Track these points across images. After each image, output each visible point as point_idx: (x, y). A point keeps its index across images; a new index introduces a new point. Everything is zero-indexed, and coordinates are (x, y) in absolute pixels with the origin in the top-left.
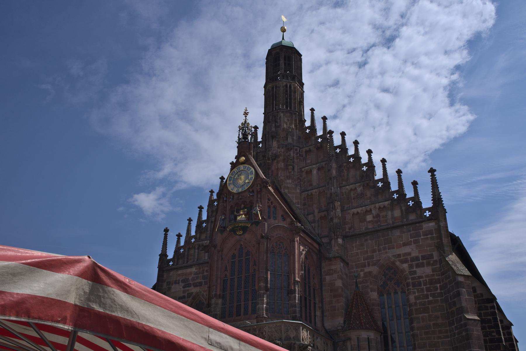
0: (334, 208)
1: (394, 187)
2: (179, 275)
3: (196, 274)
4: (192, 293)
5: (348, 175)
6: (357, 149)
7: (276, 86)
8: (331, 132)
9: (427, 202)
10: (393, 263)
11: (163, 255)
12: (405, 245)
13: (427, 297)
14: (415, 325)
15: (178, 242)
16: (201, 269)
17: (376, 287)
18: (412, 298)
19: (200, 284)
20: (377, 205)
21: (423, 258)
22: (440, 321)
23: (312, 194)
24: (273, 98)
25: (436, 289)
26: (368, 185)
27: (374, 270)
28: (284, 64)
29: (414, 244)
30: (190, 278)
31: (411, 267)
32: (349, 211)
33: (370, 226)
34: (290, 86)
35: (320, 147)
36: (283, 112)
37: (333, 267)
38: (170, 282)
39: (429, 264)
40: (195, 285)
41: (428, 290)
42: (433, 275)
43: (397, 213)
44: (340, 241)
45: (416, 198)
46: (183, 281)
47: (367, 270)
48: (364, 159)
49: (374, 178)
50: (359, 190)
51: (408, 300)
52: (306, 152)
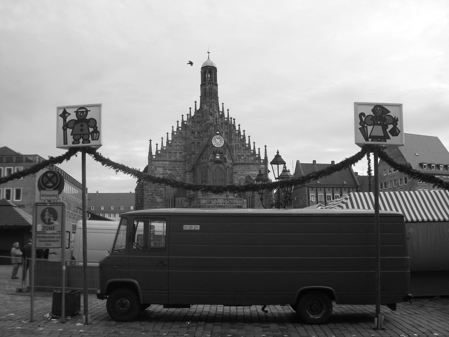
0: (233, 152)
1: (252, 149)
2: (160, 164)
3: (169, 165)
6: (239, 128)
9: (263, 157)
10: (250, 176)
11: (150, 152)
12: (254, 171)
14: (255, 198)
19: (172, 170)
27: (244, 177)
30: (166, 166)
40: (169, 170)
43: (252, 158)
45: (259, 154)
46: (163, 167)
47: (241, 177)
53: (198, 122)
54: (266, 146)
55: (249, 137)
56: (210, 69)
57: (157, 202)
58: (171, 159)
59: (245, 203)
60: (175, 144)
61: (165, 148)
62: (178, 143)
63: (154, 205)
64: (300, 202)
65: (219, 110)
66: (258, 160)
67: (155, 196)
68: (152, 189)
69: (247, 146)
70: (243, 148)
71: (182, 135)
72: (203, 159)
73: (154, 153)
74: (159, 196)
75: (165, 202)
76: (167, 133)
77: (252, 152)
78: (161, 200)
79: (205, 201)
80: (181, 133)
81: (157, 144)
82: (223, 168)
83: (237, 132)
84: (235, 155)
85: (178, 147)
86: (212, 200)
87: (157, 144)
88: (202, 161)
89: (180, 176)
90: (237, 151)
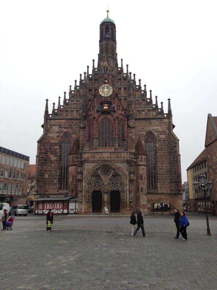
0: (131, 106)
1: (154, 103)
2: (56, 122)
3: (65, 123)
4: (63, 131)
5: (136, 94)
7: (108, 43)
8: (130, 73)
9: (166, 111)
10: (152, 132)
11: (47, 111)
12: (156, 126)
13: (163, 145)
14: (158, 154)
15: (54, 107)
16: (68, 121)
17: (144, 139)
18: (157, 145)
19: (67, 128)
20: (147, 109)
21: (163, 132)
22: (166, 154)
23: (121, 99)
24: (106, 49)
25: (166, 143)
26: (144, 99)
27: (144, 133)
28: (108, 30)
29: (160, 126)
30: (62, 124)
31: (158, 134)
32: (136, 109)
33: (143, 117)
34: (114, 45)
35: (125, 79)
36: (111, 58)
37: (132, 131)
38: (51, 125)
39: (164, 134)
40: (65, 128)
41: (163, 143)
42: (166, 138)
44: (133, 120)
45: (162, 109)
46: (58, 125)
47: (142, 133)
48: (143, 89)
49: (146, 97)
50: (140, 101)
51: (155, 146)
52: (119, 79)
53: (95, 80)
54: (169, 100)
55: (151, 91)
56: (107, 25)
57: (51, 161)
58: (67, 118)
59: (143, 160)
60: (73, 103)
61: (62, 107)
62: (75, 102)
63: (48, 163)
64: (213, 159)
65: (117, 66)
66: (161, 114)
67: (49, 154)
68: (46, 147)
69: (148, 100)
70: (143, 103)
71: (80, 94)
72: (90, 111)
73: (50, 112)
74: (53, 154)
75: (60, 161)
76: (65, 93)
77: (154, 106)
78: (56, 158)
79: (88, 156)
80: (79, 91)
81: (54, 104)
82: (112, 119)
83: (137, 87)
84: (135, 111)
85: (75, 106)
86: (96, 154)
87: (54, 104)
88: (90, 113)
89: (75, 134)
90: (138, 106)
